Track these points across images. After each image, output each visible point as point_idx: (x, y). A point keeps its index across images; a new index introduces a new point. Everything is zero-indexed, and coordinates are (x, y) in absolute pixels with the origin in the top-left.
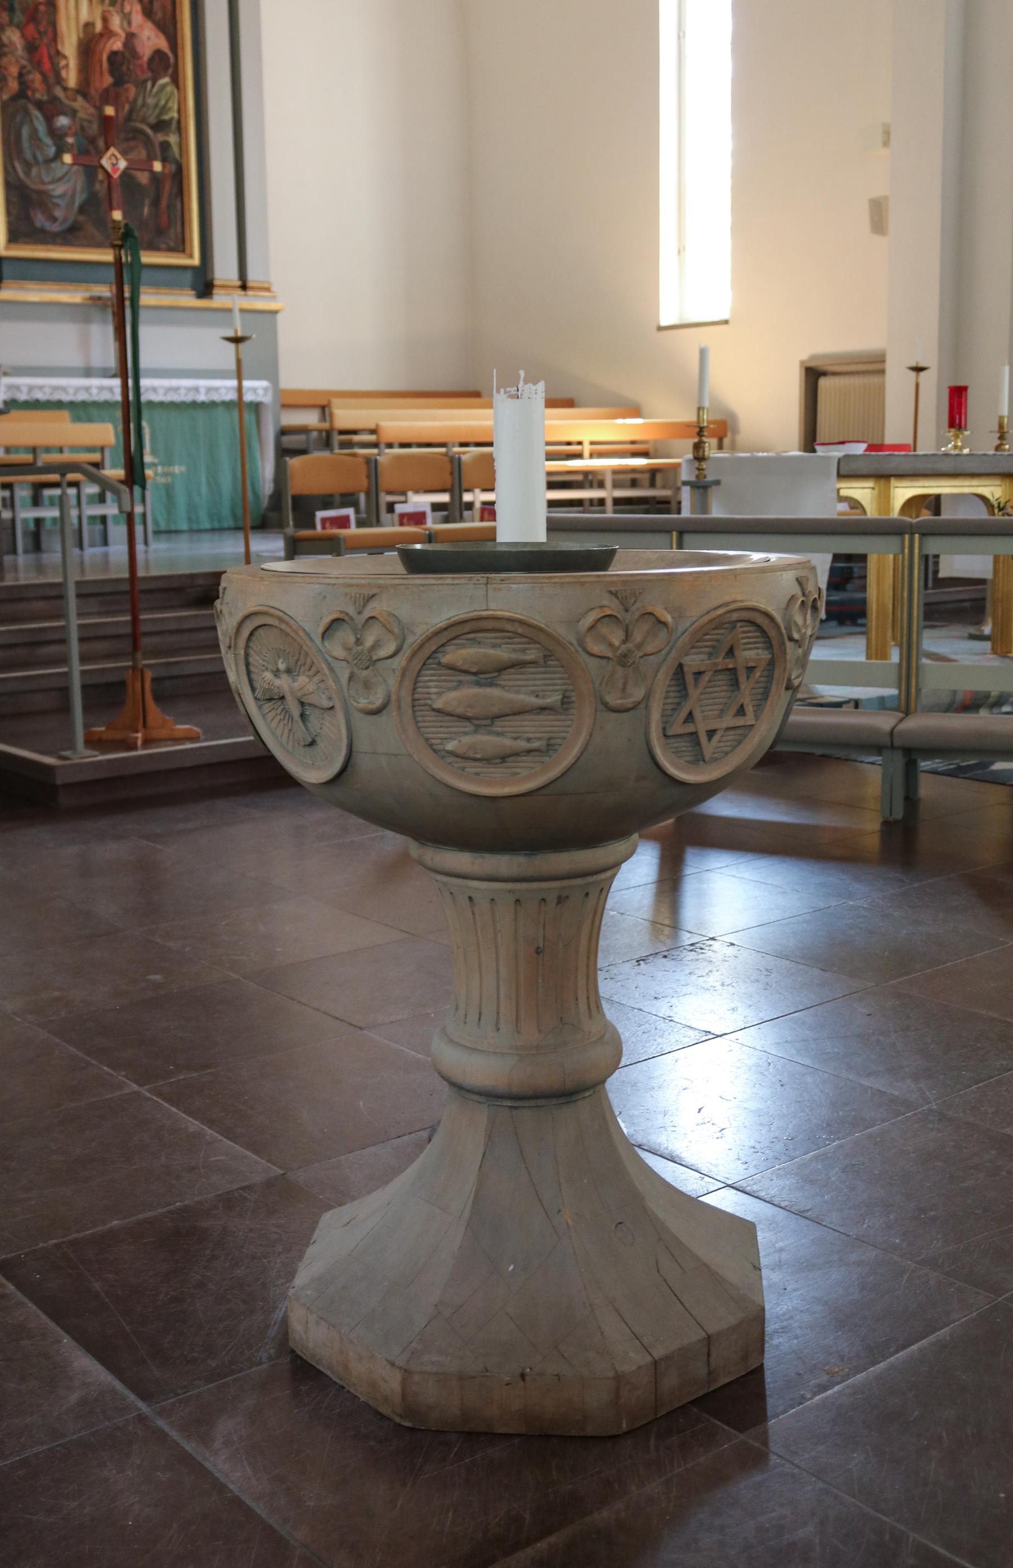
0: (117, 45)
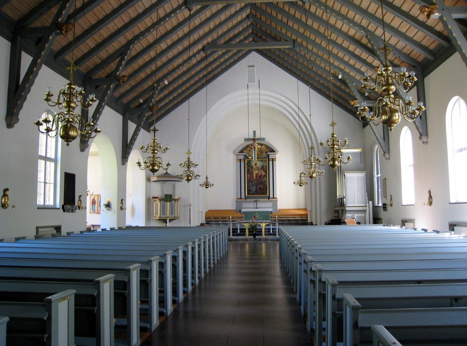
0: (260, 175)
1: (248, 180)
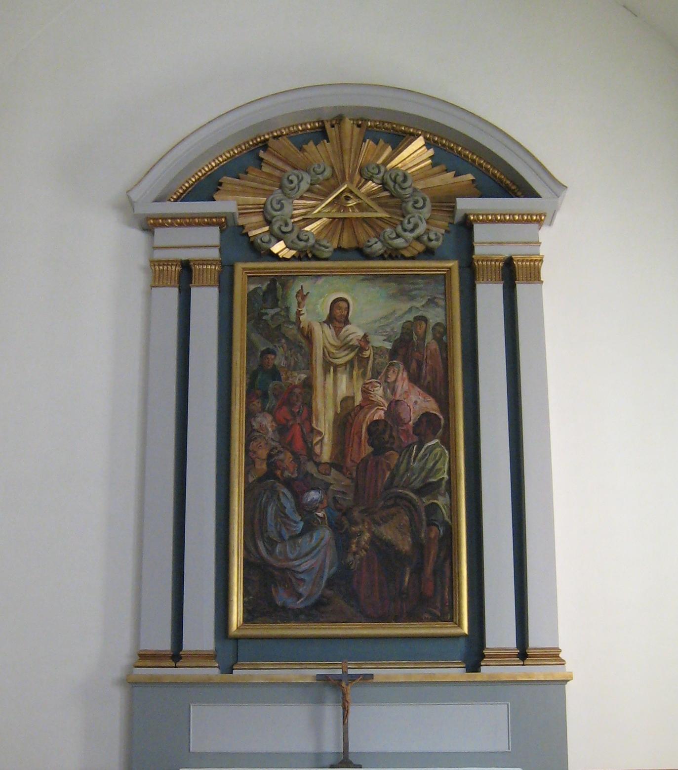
0: (380, 414)
1: (262, 467)
